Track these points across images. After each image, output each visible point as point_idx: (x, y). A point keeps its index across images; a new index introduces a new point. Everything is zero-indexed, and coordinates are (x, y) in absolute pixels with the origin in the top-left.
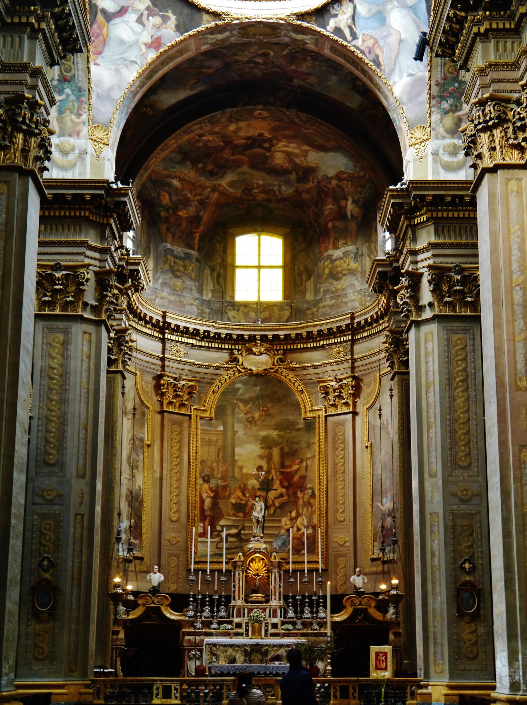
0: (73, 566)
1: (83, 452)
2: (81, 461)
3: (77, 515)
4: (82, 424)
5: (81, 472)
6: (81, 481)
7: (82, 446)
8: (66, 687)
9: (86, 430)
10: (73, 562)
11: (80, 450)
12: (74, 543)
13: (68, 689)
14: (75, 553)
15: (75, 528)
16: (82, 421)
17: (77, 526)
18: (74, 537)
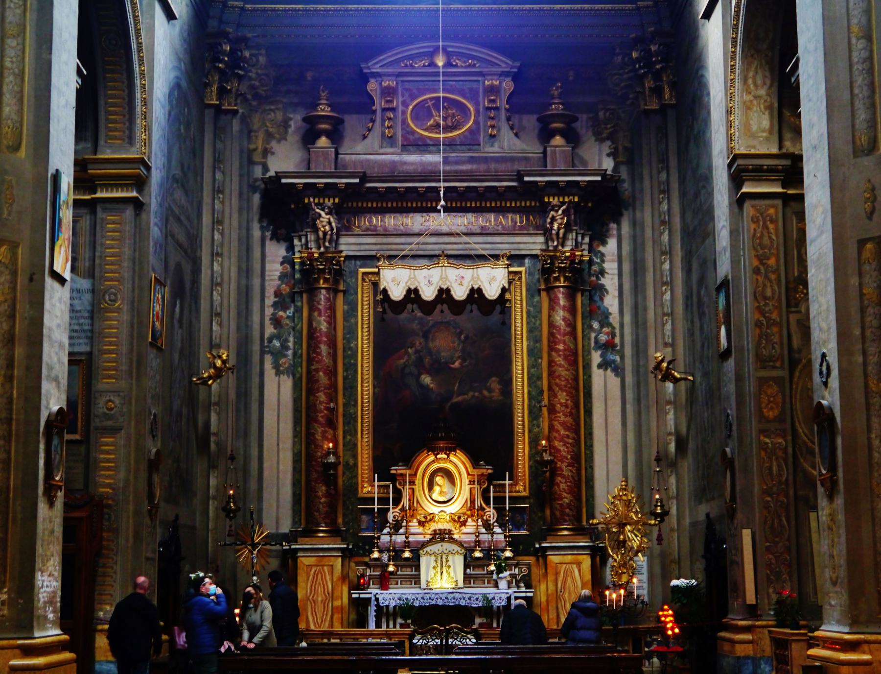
0: (865, 364)
1: (866, 92)
2: (862, 115)
3: (862, 243)
4: (855, 29)
5: (864, 140)
6: (866, 161)
7: (859, 80)
8: (865, 647)
9: (869, 38)
10: (865, 354)
11: (856, 91)
12: (863, 310)
13: (871, 653)
14: (868, 333)
15: (860, 275)
16: (854, 21)
17: (866, 267)
18: (862, 295)
